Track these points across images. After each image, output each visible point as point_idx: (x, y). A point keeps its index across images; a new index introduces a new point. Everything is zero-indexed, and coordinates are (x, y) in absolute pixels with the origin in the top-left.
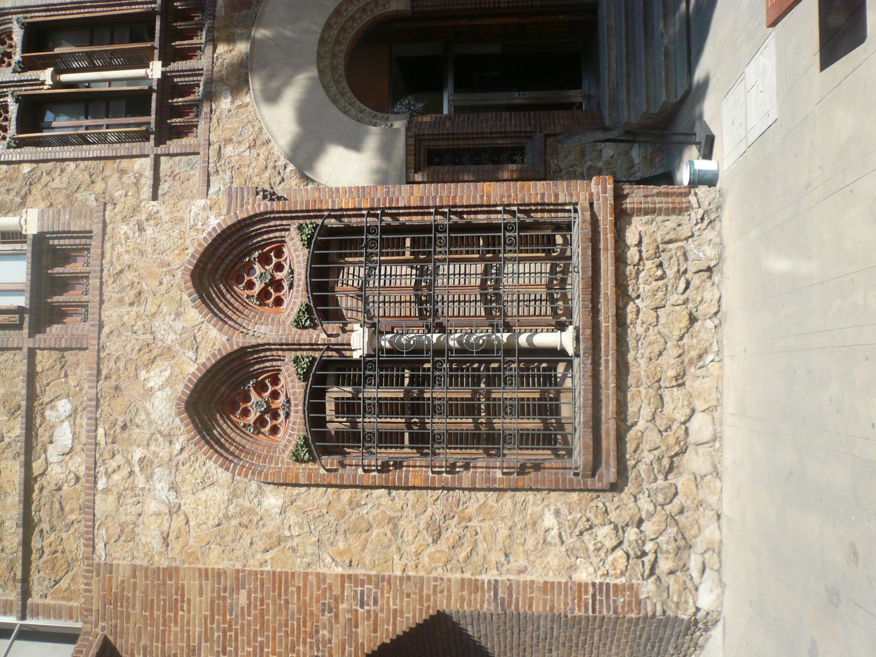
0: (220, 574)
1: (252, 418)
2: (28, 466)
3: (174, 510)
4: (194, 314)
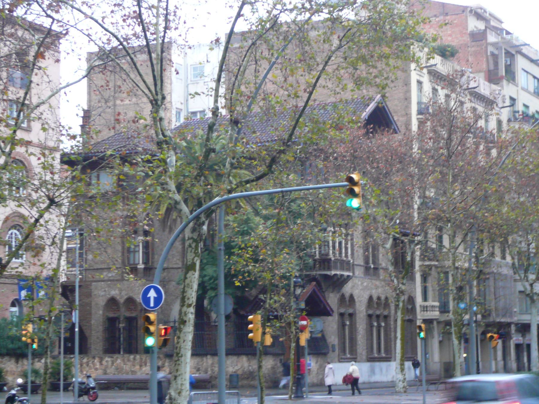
0: (91, 304)
1: (113, 307)
2: (105, 269)
3: (99, 296)
4: (126, 297)
